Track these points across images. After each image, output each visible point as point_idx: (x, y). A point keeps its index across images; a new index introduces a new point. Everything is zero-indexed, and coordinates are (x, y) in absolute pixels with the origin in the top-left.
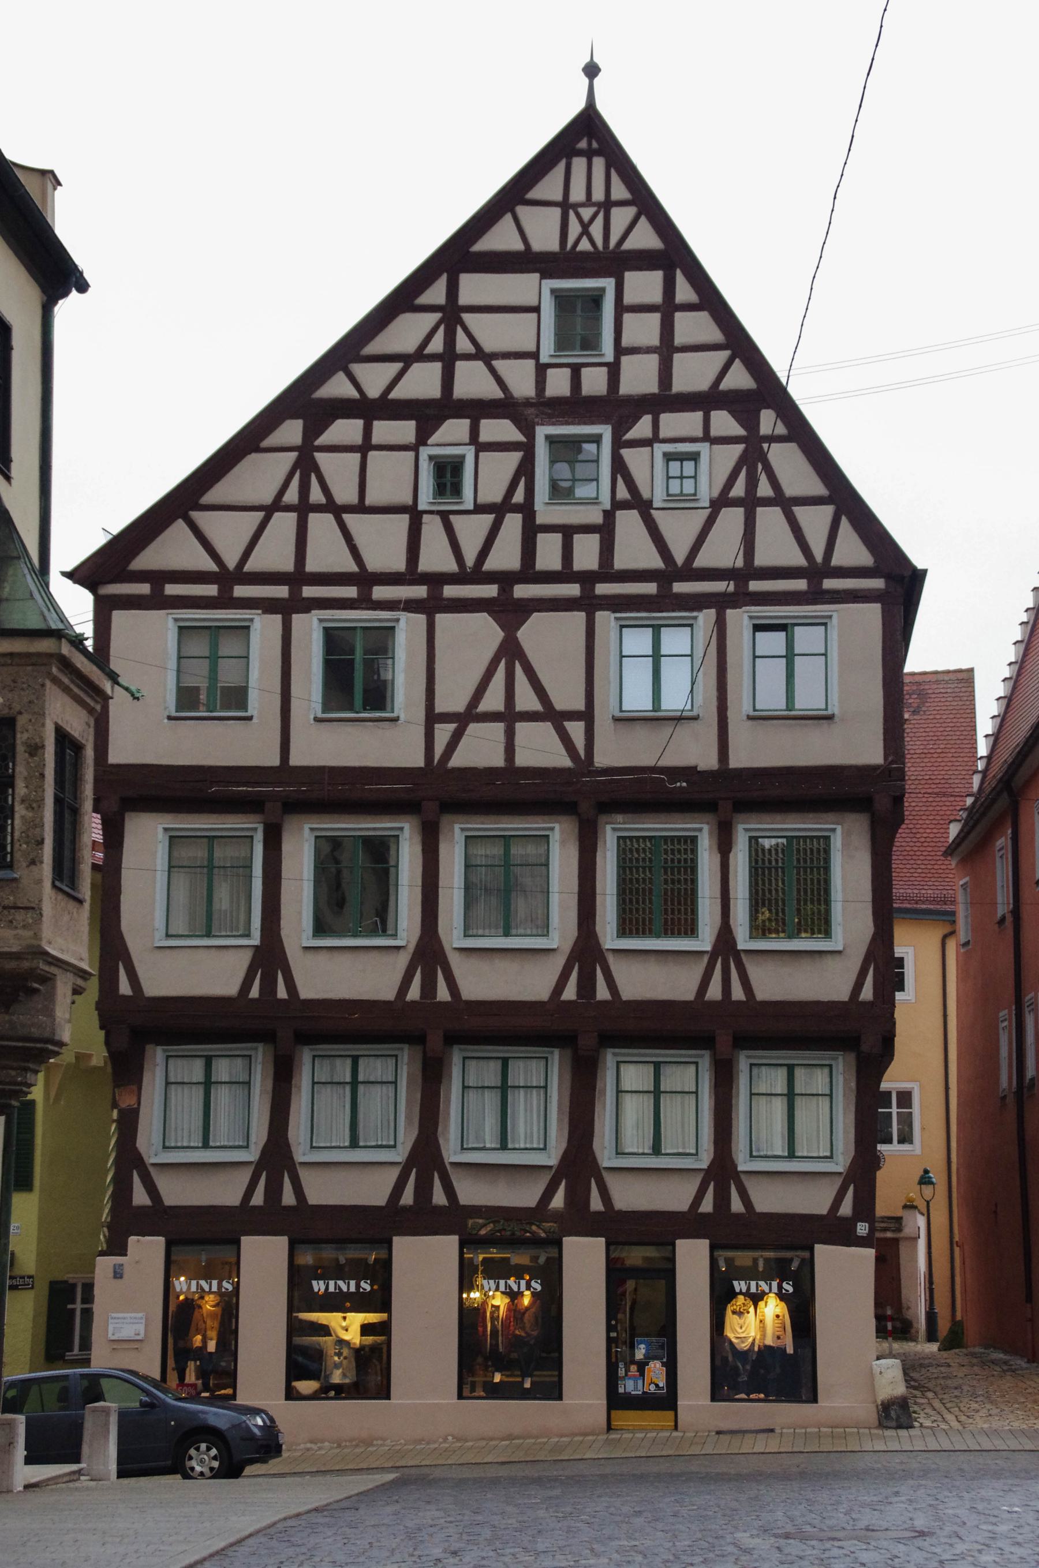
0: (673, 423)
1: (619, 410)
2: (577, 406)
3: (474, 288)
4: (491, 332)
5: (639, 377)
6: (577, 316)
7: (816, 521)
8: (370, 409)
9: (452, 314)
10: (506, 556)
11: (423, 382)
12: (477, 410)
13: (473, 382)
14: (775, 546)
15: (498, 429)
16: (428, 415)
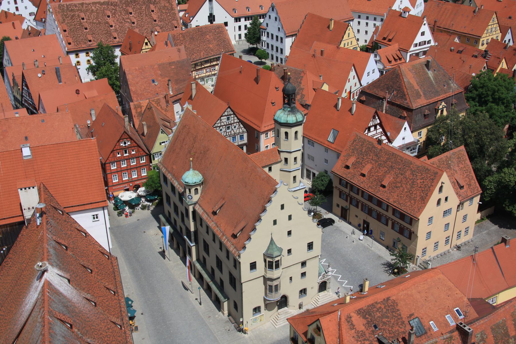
0: (235, 124)
1: (231, 124)
2: (229, 124)
3: (222, 118)
4: (223, 121)
5: (232, 122)
6: (228, 119)
7: (243, 129)
8: (216, 127)
9: (221, 120)
10: (225, 135)
11: (219, 125)
12: (223, 126)
13: (222, 124)
14: (241, 131)
15: (224, 127)
16: (219, 127)
